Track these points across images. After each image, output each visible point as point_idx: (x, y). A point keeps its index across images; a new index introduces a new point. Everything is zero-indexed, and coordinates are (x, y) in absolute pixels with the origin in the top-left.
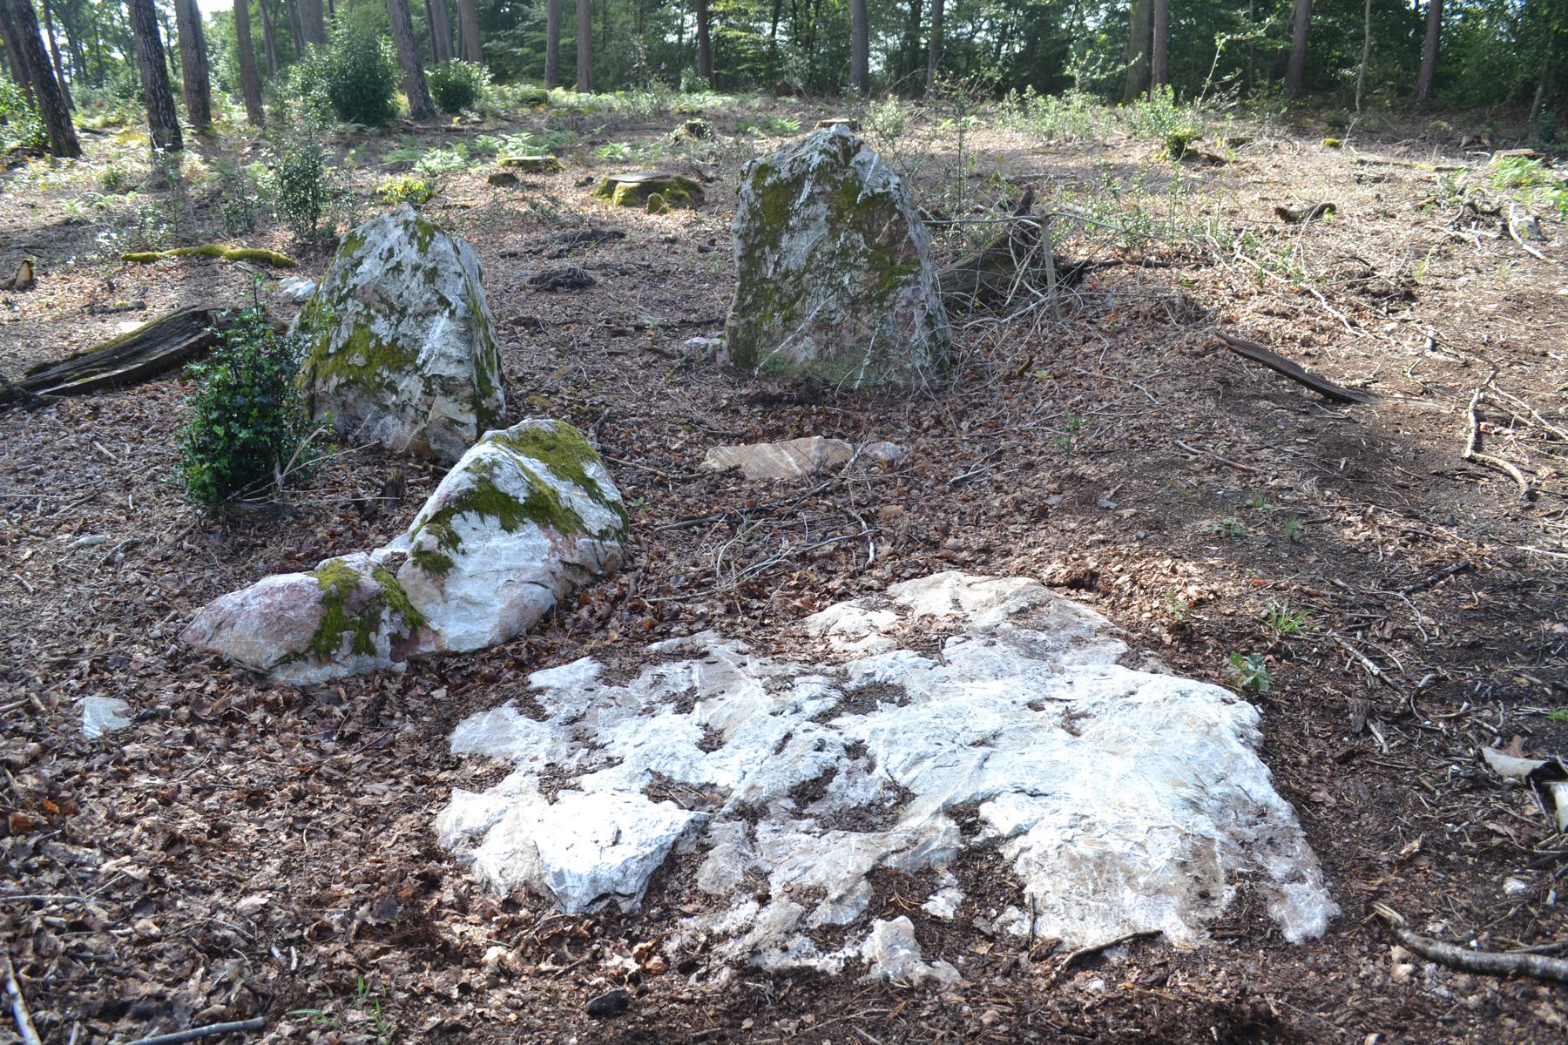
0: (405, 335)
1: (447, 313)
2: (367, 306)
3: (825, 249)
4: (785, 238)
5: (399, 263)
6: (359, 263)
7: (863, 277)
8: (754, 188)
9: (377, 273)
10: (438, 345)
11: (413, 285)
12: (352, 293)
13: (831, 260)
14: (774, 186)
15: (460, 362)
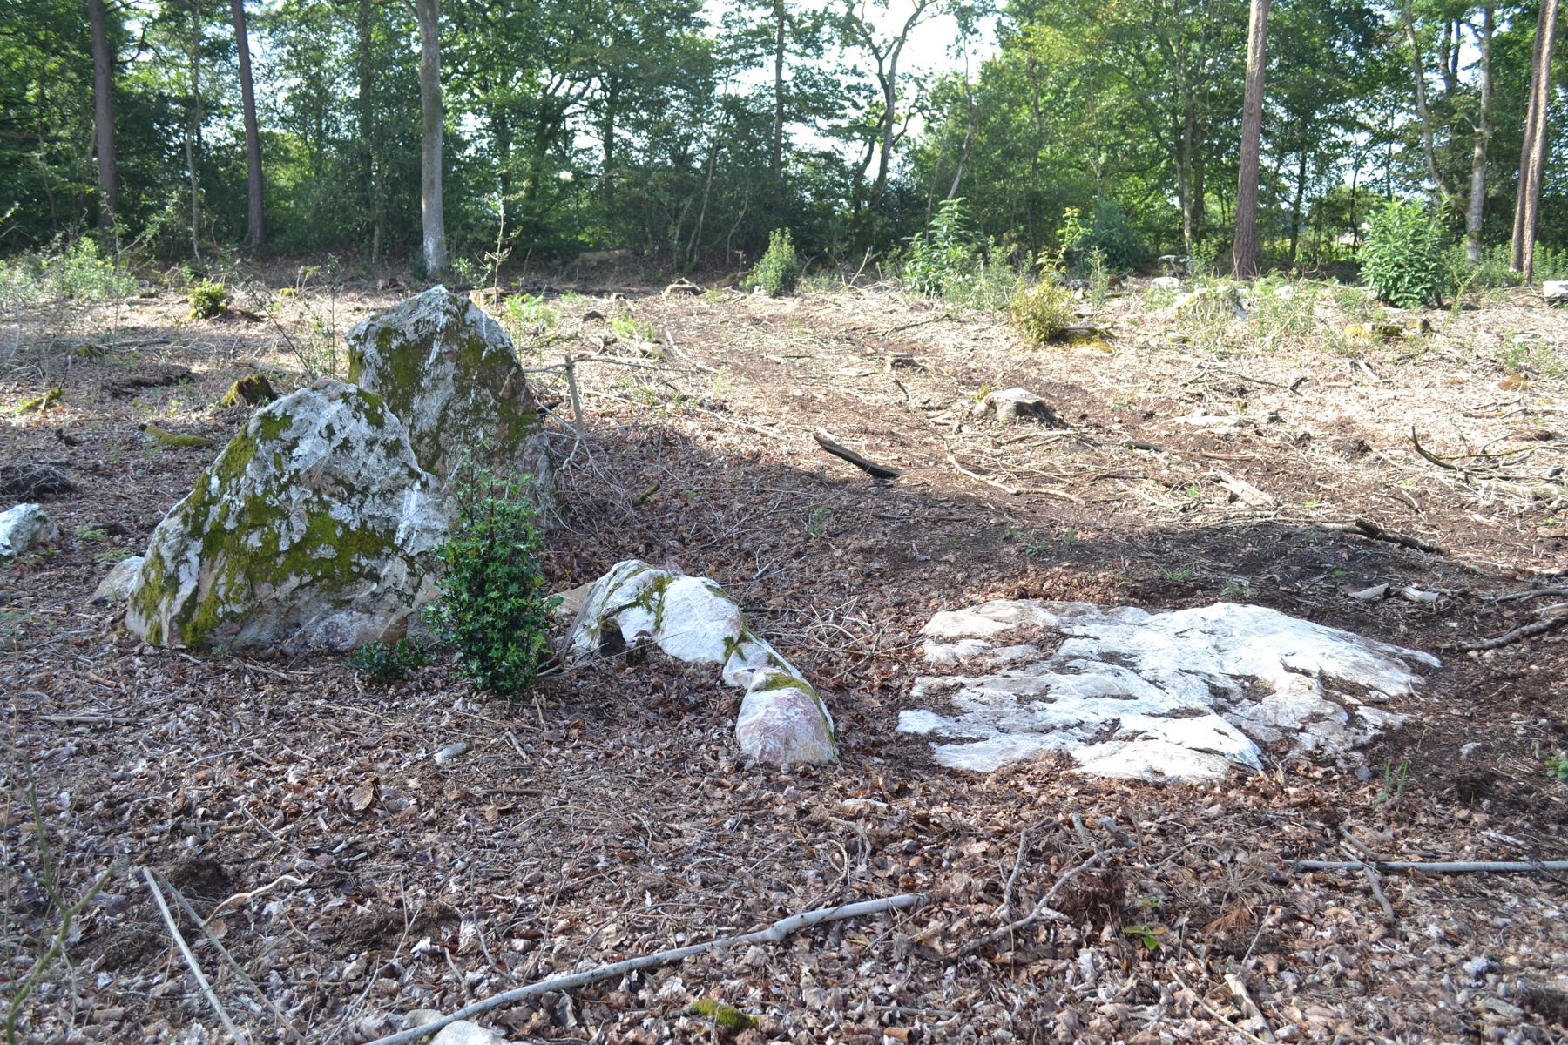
0: (372, 517)
1: (418, 486)
2: (317, 492)
3: (458, 407)
4: (417, 400)
5: (346, 440)
6: (295, 443)
7: (495, 430)
8: (380, 352)
9: (323, 453)
10: (418, 521)
11: (372, 460)
12: (295, 479)
13: (464, 418)
14: (402, 348)
15: (445, 534)
